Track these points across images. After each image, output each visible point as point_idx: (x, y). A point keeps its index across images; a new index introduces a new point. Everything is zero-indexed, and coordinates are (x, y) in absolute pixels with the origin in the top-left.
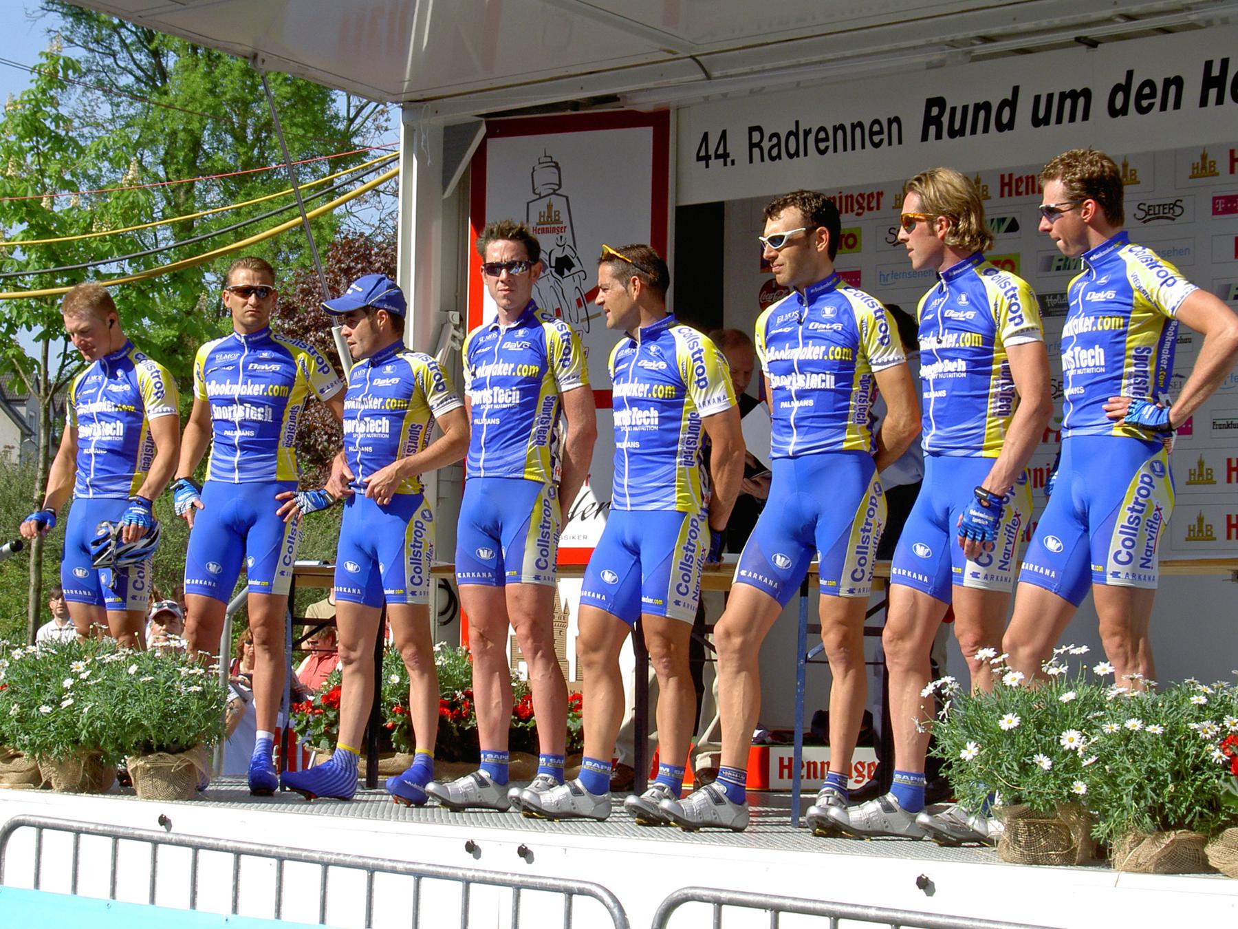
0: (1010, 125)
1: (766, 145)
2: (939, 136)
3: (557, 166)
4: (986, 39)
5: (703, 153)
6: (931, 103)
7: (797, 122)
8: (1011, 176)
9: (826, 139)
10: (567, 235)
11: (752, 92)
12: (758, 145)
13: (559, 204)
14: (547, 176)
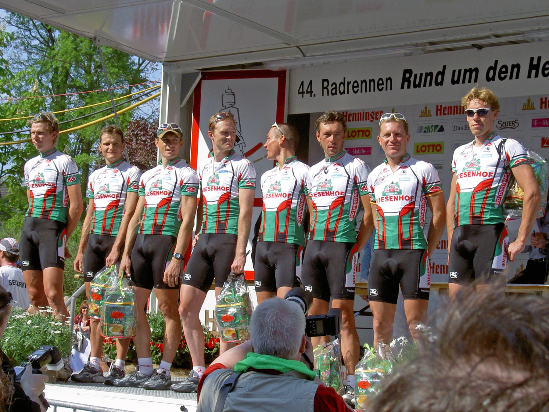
1: (330, 88)
3: (234, 94)
4: (432, 44)
5: (301, 91)
7: (344, 78)
8: (441, 106)
9: (358, 86)
11: (324, 63)
12: (326, 88)
13: (234, 111)
14: (229, 98)
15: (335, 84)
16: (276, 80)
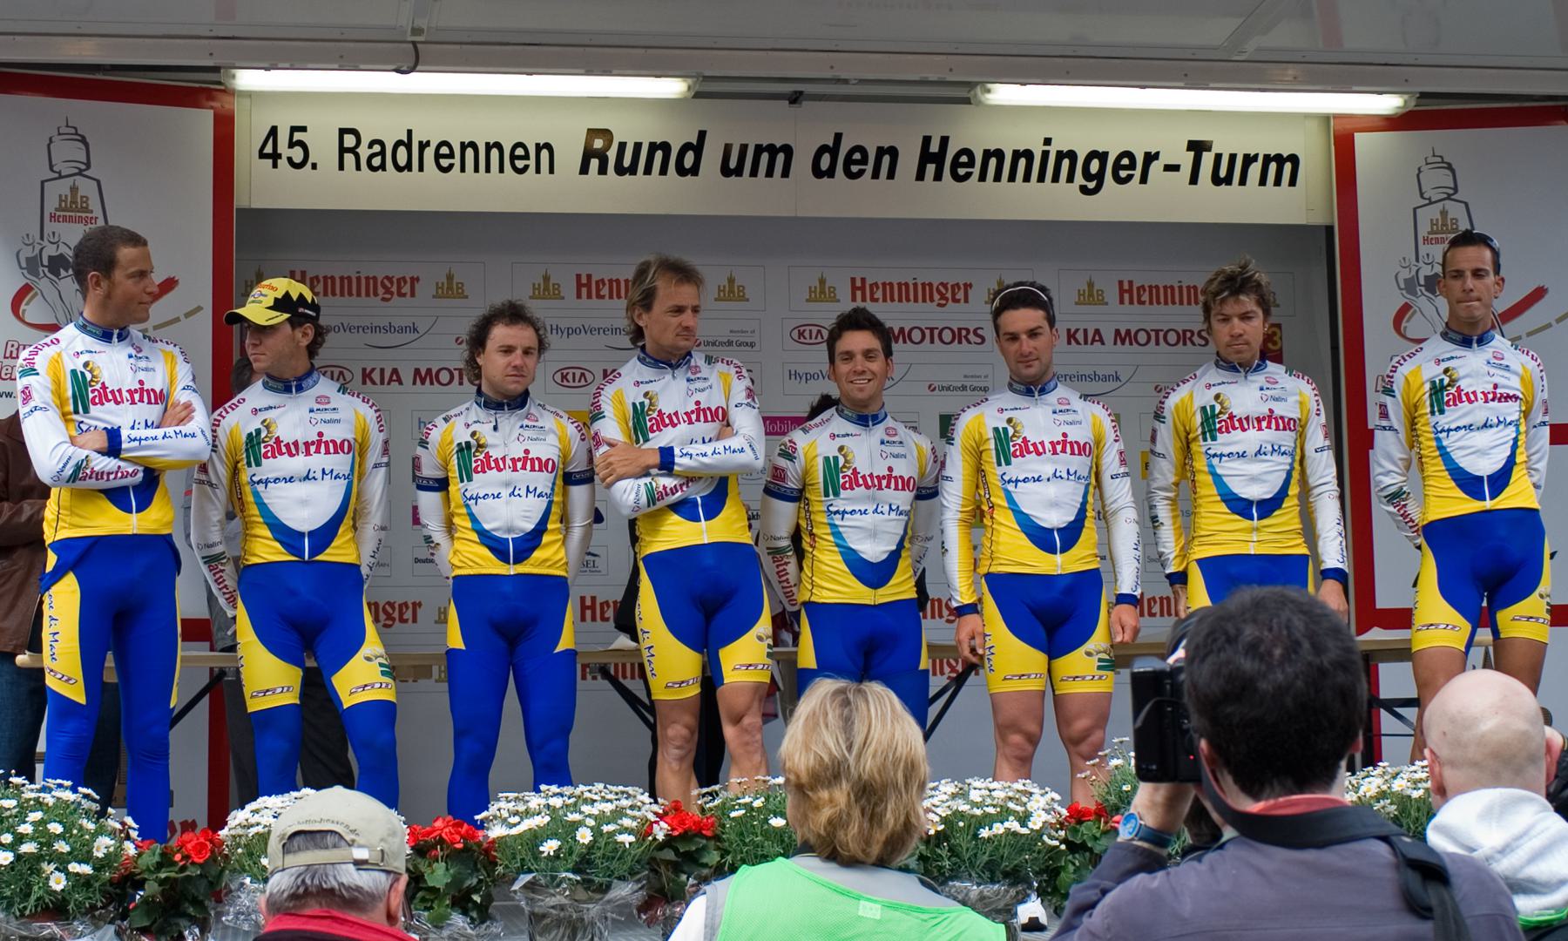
0: (694, 171)
1: (364, 152)
2: (603, 170)
3: (83, 140)
5: (269, 149)
7: (410, 132)
9: (451, 155)
13: (86, 188)
16: (202, 121)
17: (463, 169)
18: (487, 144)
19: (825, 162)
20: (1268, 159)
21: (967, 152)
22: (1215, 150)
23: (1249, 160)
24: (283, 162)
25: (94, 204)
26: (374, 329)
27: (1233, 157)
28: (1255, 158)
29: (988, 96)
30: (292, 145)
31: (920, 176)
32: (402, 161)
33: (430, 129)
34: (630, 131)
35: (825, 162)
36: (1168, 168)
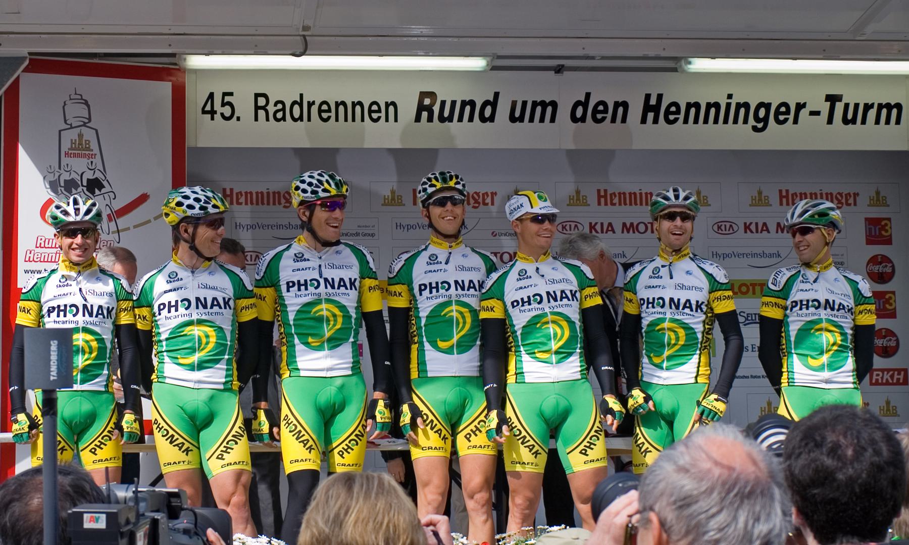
0: (492, 119)
1: (271, 109)
2: (430, 119)
3: (86, 103)
5: (208, 108)
6: (423, 95)
7: (301, 95)
10: (97, 161)
13: (88, 134)
14: (76, 111)
15: (282, 103)
16: (165, 88)
17: (337, 120)
18: (353, 103)
19: (579, 112)
20: (880, 107)
21: (676, 104)
22: (845, 100)
23: (868, 107)
24: (217, 117)
25: (94, 145)
26: (279, 227)
27: (857, 106)
28: (872, 106)
29: (690, 66)
30: (223, 104)
31: (644, 121)
32: (297, 114)
33: (315, 94)
34: (446, 93)
35: (579, 112)
36: (813, 113)
